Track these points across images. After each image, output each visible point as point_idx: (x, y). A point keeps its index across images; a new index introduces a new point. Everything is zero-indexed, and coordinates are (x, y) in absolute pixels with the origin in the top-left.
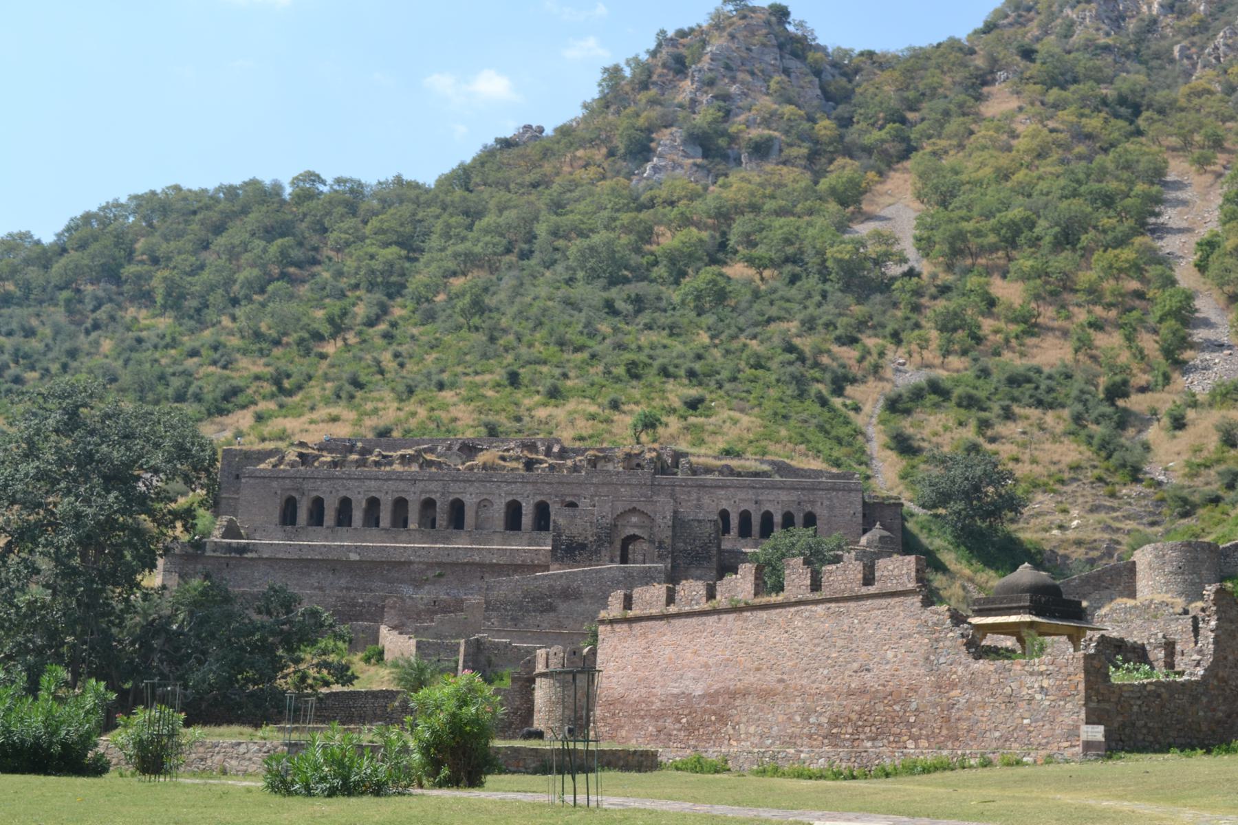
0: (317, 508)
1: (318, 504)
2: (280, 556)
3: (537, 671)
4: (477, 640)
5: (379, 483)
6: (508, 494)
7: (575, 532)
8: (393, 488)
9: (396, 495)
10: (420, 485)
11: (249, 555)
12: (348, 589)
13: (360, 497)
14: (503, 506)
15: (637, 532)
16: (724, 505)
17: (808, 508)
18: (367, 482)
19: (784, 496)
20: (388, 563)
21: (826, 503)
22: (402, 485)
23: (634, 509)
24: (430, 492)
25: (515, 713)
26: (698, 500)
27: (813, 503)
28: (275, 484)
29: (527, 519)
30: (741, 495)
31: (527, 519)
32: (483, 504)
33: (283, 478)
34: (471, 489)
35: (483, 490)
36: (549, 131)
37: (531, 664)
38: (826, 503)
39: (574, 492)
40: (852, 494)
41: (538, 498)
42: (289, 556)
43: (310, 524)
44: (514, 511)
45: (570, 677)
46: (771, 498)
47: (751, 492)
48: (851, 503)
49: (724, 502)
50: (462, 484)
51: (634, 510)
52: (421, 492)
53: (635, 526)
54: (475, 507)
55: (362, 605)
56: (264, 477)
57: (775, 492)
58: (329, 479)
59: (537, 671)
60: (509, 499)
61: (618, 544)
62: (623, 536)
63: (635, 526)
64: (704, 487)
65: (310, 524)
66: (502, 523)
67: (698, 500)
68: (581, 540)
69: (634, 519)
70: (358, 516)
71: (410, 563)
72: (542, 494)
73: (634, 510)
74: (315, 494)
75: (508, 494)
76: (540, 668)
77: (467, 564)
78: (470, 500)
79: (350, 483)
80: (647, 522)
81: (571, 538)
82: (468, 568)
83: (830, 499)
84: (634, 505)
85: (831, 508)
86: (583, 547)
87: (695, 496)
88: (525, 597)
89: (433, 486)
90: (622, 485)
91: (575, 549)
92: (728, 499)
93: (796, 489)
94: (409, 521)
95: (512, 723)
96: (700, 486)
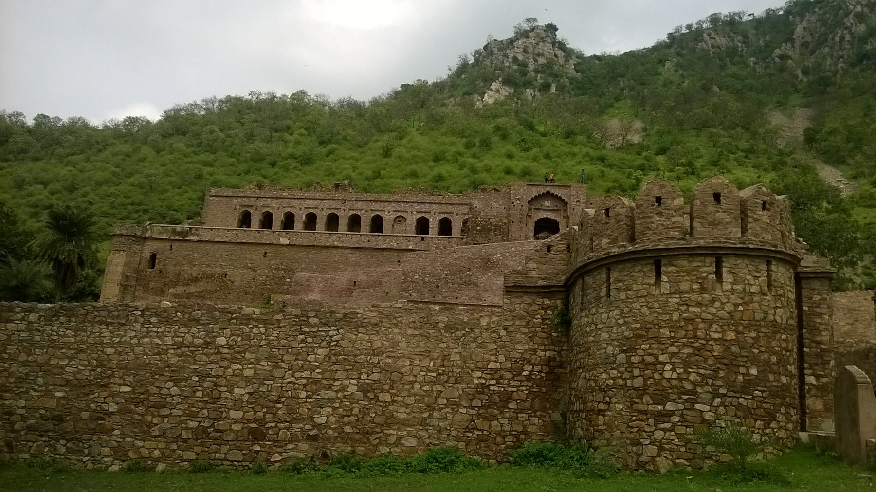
0: (267, 221)
9: (330, 212)
13: (301, 212)
14: (415, 221)
15: (550, 215)
22: (334, 204)
23: (548, 192)
25: (516, 373)
28: (235, 201)
35: (399, 209)
36: (430, 83)
41: (443, 216)
44: (422, 226)
50: (383, 204)
52: (350, 209)
54: (392, 223)
68: (495, 221)
69: (547, 204)
78: (388, 216)
79: (294, 202)
82: (386, 253)
84: (548, 189)
89: (359, 205)
91: (489, 230)
95: (507, 398)
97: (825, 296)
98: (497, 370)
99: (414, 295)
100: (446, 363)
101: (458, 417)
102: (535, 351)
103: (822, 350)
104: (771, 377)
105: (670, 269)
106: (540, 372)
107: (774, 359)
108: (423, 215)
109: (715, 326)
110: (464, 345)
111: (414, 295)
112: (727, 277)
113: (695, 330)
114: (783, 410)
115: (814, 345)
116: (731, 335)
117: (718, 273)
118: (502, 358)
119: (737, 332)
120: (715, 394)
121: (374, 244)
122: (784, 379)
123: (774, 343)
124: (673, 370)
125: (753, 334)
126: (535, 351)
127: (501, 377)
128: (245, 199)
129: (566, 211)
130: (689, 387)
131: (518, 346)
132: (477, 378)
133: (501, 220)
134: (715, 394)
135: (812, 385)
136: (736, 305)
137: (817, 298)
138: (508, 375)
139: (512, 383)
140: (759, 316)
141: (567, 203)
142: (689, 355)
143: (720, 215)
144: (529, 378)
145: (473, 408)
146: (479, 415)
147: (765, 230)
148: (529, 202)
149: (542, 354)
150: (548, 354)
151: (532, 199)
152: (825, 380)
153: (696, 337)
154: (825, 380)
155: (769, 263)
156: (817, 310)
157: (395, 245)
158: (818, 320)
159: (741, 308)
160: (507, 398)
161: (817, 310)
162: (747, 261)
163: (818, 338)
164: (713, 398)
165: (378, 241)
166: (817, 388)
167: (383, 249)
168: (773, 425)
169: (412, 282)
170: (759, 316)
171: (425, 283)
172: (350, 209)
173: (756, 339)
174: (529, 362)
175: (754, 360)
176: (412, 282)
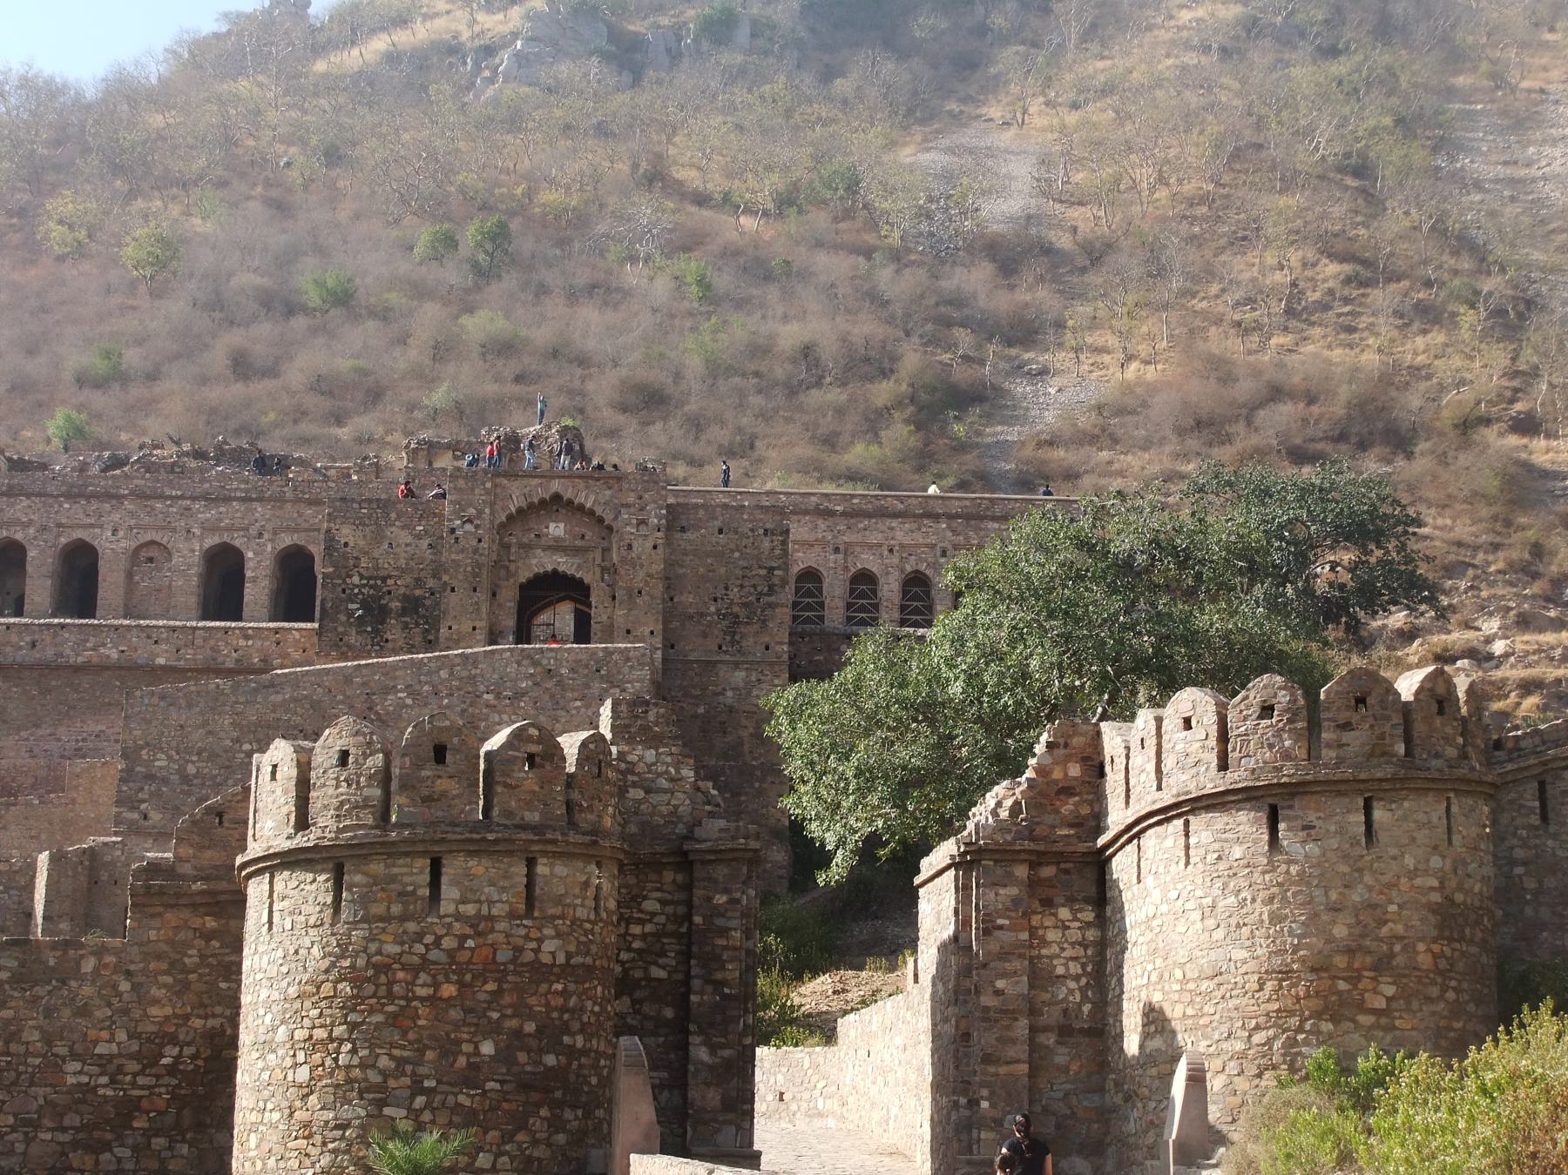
3: (254, 849)
4: (92, 853)
15: (564, 564)
19: (902, 533)
23: (557, 497)
24: (9, 524)
25: (148, 1060)
29: (258, 588)
31: (258, 588)
32: (147, 555)
34: (116, 517)
37: (229, 821)
41: (287, 540)
45: (416, 874)
46: (874, 538)
50: (95, 505)
51: (555, 505)
53: (557, 547)
54: (123, 563)
59: (254, 849)
60: (212, 541)
61: (509, 597)
62: (524, 576)
63: (557, 547)
66: (193, 601)
69: (556, 529)
73: (555, 505)
75: (214, 529)
76: (269, 827)
78: (112, 545)
81: (378, 579)
84: (556, 486)
93: (936, 517)
97: (738, 895)
98: (111, 1057)
99: (155, 816)
100: (13, 1047)
101: (35, 1149)
102: (187, 1017)
103: (724, 997)
104: (522, 1057)
105: (358, 878)
106: (194, 1057)
107: (530, 1027)
108: (226, 538)
109: (423, 978)
110: (48, 1012)
111: (155, 816)
112: (449, 892)
113: (390, 984)
114: (544, 1112)
115: (709, 988)
116: (449, 990)
117: (435, 884)
118: (122, 1036)
119: (461, 984)
120: (417, 1088)
121: (50, 653)
122: (550, 1060)
123: (532, 1001)
124: (354, 1051)
125: (491, 986)
126: (187, 1017)
127: (120, 1070)
129: (606, 551)
130: (374, 1077)
131: (154, 1011)
132: (74, 1074)
133: (419, 582)
134: (417, 1088)
135: (702, 1062)
136: (463, 938)
137: (721, 899)
138: (133, 1066)
139: (141, 1081)
140: (503, 956)
141: (610, 528)
142: (378, 1026)
143: (442, 784)
144: (172, 1070)
145: (64, 1130)
146: (75, 1145)
147: (529, 805)
148: (502, 526)
149: (197, 1023)
150: (211, 1023)
151: (510, 518)
152: (726, 1053)
153: (391, 996)
154: (726, 1053)
155: (531, 863)
156: (720, 922)
157: (114, 655)
158: (721, 942)
159: (470, 943)
160: (127, 1109)
161: (720, 922)
162: (486, 862)
163: (719, 976)
164: (413, 1096)
165: (70, 638)
166: (711, 1068)
167: (77, 669)
168: (520, 1137)
169: (150, 777)
170: (503, 956)
171: (186, 779)
173: (498, 993)
174: (173, 1040)
175: (494, 1030)
176: (150, 777)
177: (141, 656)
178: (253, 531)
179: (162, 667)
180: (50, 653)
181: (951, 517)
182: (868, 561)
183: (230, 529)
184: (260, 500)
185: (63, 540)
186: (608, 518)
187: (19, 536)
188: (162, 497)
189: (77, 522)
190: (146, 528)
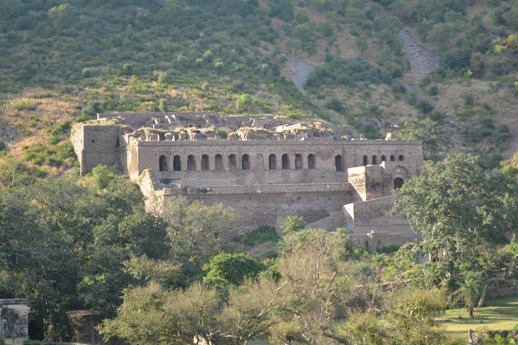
1: (177, 159)
2: (224, 193)
5: (208, 147)
6: (270, 151)
7: (374, 177)
8: (215, 149)
10: (228, 148)
11: (209, 193)
12: (258, 207)
16: (365, 153)
17: (400, 153)
18: (202, 147)
20: (275, 194)
21: (408, 151)
22: (219, 148)
24: (232, 151)
26: (355, 151)
27: (402, 151)
28: (155, 149)
30: (373, 148)
33: (159, 146)
35: (258, 150)
38: (408, 151)
39: (300, 149)
40: (418, 147)
41: (284, 153)
42: (227, 193)
43: (175, 170)
46: (385, 149)
47: (376, 147)
48: (418, 150)
49: (365, 152)
50: (248, 147)
52: (229, 151)
53: (399, 173)
55: (266, 215)
56: (149, 146)
57: (387, 146)
58: (182, 145)
60: (270, 153)
63: (399, 173)
64: (357, 145)
65: (175, 170)
67: (355, 151)
68: (377, 181)
69: (398, 171)
70: (198, 164)
71: (285, 193)
72: (286, 151)
74: (176, 154)
77: (311, 192)
78: (252, 154)
79: (193, 148)
80: (404, 171)
82: (311, 194)
83: (409, 149)
85: (410, 153)
86: (378, 184)
87: (353, 150)
88: (371, 210)
90: (321, 145)
91: (375, 185)
92: (367, 150)
93: (395, 145)
94: (224, 166)
96: (355, 144)
99: (360, 223)
108: (273, 153)
111: (360, 223)
128: (161, 148)
172: (229, 151)
177: (319, 190)
178: (278, 151)
179: (324, 192)
180: (305, 190)
181: (398, 144)
182: (384, 154)
183: (273, 151)
184: (279, 145)
185: (243, 154)
186: (408, 168)
187: (234, 154)
188: (261, 145)
189: (245, 150)
190: (258, 151)
